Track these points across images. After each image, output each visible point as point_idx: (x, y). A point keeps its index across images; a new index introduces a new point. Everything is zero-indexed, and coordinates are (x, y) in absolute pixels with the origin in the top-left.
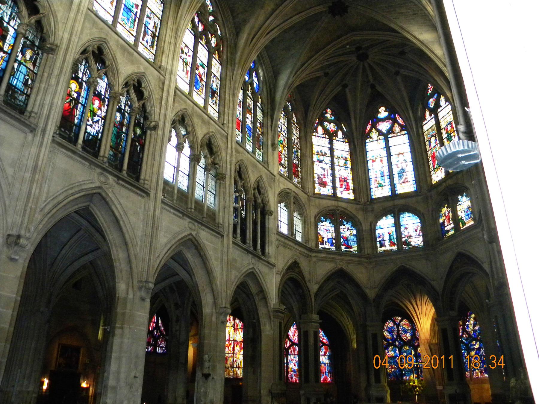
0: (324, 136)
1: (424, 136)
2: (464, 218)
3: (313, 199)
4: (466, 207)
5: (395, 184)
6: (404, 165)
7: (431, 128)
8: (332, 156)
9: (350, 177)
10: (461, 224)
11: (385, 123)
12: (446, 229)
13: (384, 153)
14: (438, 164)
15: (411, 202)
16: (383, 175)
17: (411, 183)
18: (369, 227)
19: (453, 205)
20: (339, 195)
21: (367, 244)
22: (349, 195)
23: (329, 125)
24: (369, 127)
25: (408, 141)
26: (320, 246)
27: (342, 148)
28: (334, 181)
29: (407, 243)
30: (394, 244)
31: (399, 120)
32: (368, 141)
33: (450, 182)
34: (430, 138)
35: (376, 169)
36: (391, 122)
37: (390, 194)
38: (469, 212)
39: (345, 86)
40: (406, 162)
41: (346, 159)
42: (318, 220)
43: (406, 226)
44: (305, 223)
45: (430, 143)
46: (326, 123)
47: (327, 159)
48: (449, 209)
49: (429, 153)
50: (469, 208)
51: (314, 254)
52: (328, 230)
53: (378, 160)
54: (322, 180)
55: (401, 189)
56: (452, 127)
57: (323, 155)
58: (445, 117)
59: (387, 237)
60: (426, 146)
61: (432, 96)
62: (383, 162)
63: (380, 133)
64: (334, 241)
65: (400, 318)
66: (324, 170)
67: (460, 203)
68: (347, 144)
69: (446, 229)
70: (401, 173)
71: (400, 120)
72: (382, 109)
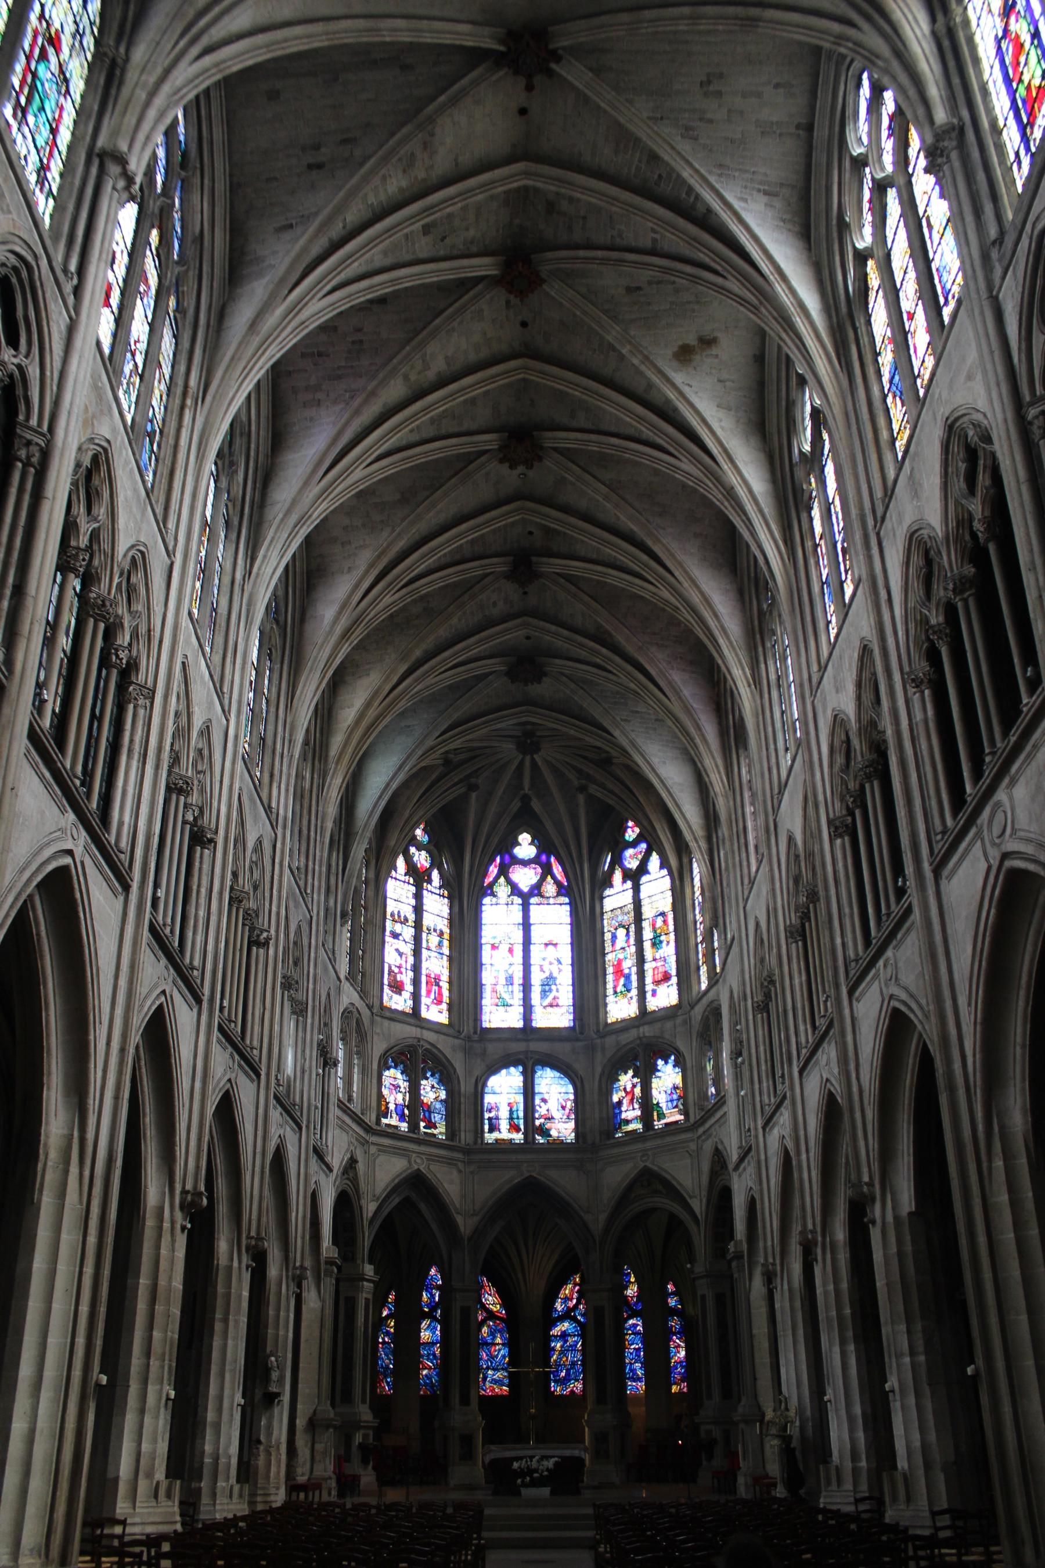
1: (602, 920)
2: (663, 1105)
3: (378, 1019)
4: (671, 1086)
5: (531, 1006)
6: (555, 969)
7: (621, 908)
8: (418, 925)
9: (445, 977)
10: (655, 1114)
11: (526, 870)
12: (624, 1116)
13: (518, 936)
14: (624, 985)
15: (562, 1049)
16: (510, 981)
17: (564, 1009)
18: (472, 1090)
19: (646, 1074)
20: (424, 1014)
21: (465, 1124)
22: (436, 1013)
23: (417, 853)
24: (493, 870)
25: (568, 920)
26: (384, 1121)
27: (437, 908)
28: (416, 982)
29: (544, 1132)
30: (518, 1130)
31: (555, 871)
32: (487, 900)
33: (646, 1031)
34: (616, 929)
35: (497, 967)
36: (539, 870)
37: (520, 1024)
38: (675, 1097)
39: (472, 788)
40: (560, 963)
41: (441, 934)
42: (384, 1066)
43: (546, 1097)
44: (364, 1071)
45: (614, 937)
46: (413, 850)
47: (408, 932)
48: (636, 1080)
49: (609, 957)
50: (675, 1088)
51: (374, 1139)
52: (397, 1087)
54: (395, 977)
55: (543, 1019)
56: (665, 922)
57: (401, 923)
58: (654, 898)
59: (504, 1114)
60: (603, 941)
61: (634, 844)
62: (515, 953)
63: (515, 890)
64: (406, 1112)
66: (401, 954)
67: (658, 1074)
68: (446, 900)
69: (624, 1116)
70: (549, 983)
71: (557, 870)
72: (525, 838)
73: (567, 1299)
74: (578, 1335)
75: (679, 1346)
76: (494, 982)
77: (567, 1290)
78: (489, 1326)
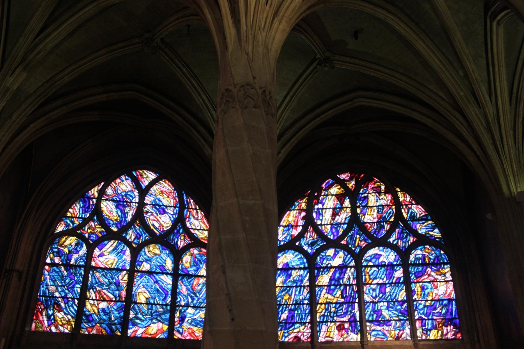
65: (152, 176)
73: (289, 226)
74: (304, 269)
75: (435, 281)
77: (291, 216)
78: (192, 255)
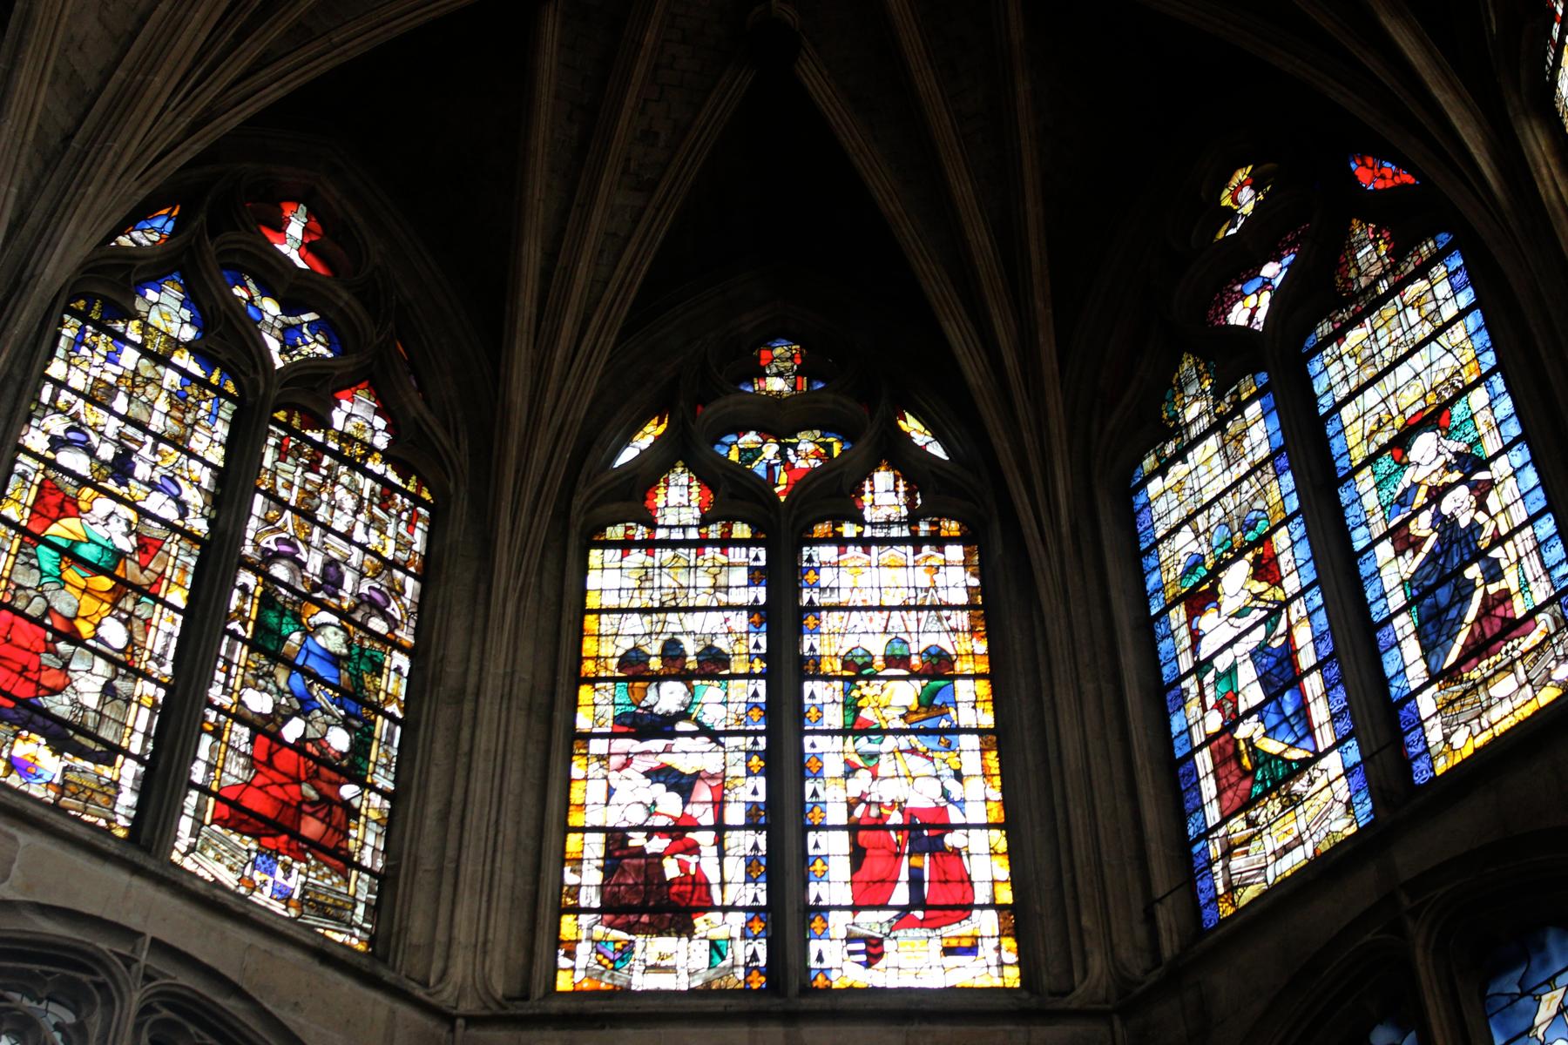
0: (715, 531)
6: (1458, 503)
8: (786, 669)
13: (1281, 491)
16: (1280, 672)
17: (1544, 621)
32: (1149, 463)
53: (1237, 581)
57: (686, 677)
76: (1214, 722)
